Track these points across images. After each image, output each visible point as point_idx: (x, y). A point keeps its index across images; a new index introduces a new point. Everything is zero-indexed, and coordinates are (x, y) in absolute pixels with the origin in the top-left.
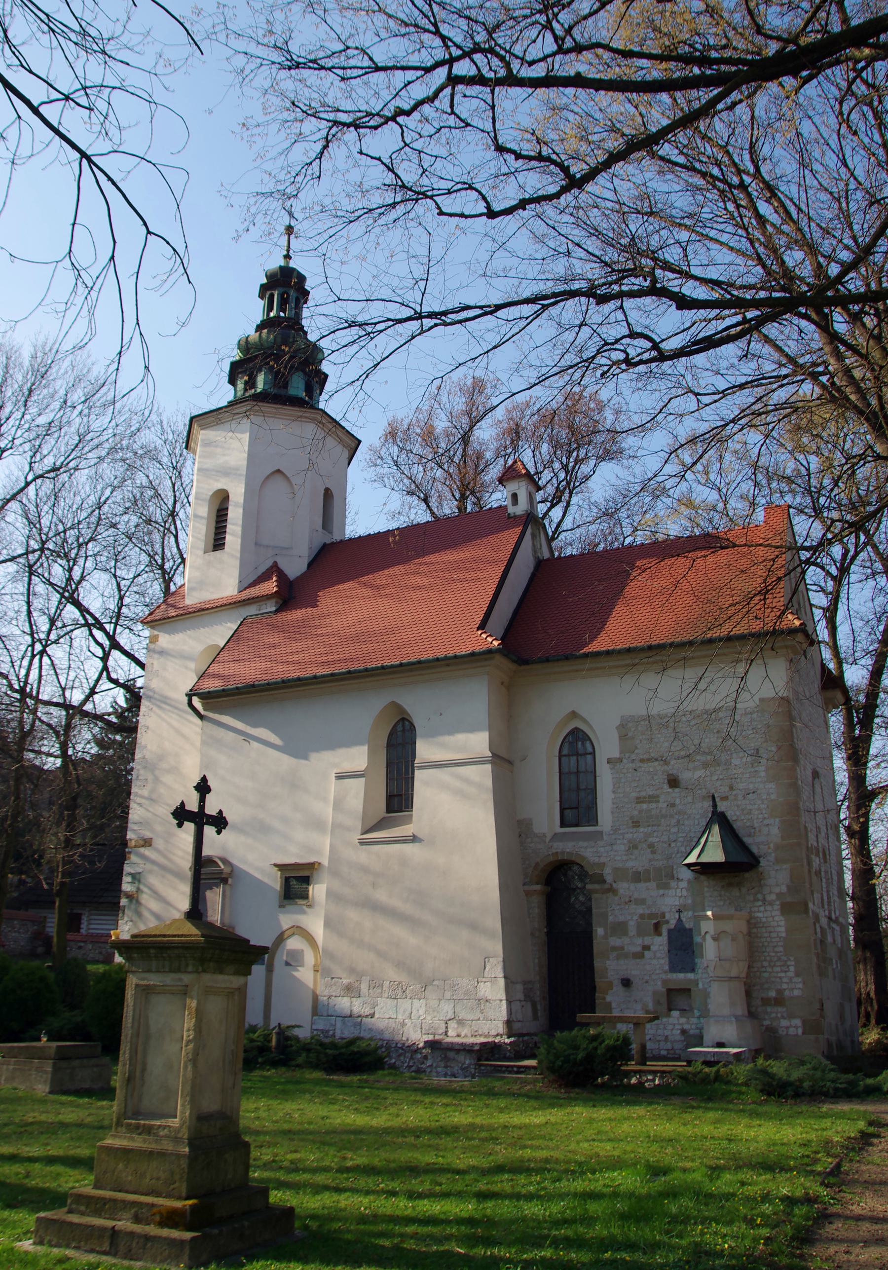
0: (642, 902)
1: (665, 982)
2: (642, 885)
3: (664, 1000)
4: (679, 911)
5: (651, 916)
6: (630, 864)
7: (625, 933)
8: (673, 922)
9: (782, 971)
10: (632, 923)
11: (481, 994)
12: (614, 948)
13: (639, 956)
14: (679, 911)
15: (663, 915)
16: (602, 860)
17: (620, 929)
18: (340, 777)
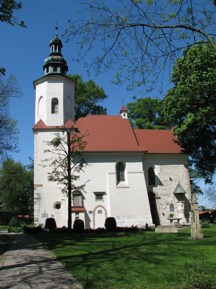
0: (164, 199)
2: (165, 196)
3: (169, 216)
6: (163, 193)
11: (147, 217)
12: (161, 208)
13: (165, 209)
17: (161, 204)
18: (109, 174)
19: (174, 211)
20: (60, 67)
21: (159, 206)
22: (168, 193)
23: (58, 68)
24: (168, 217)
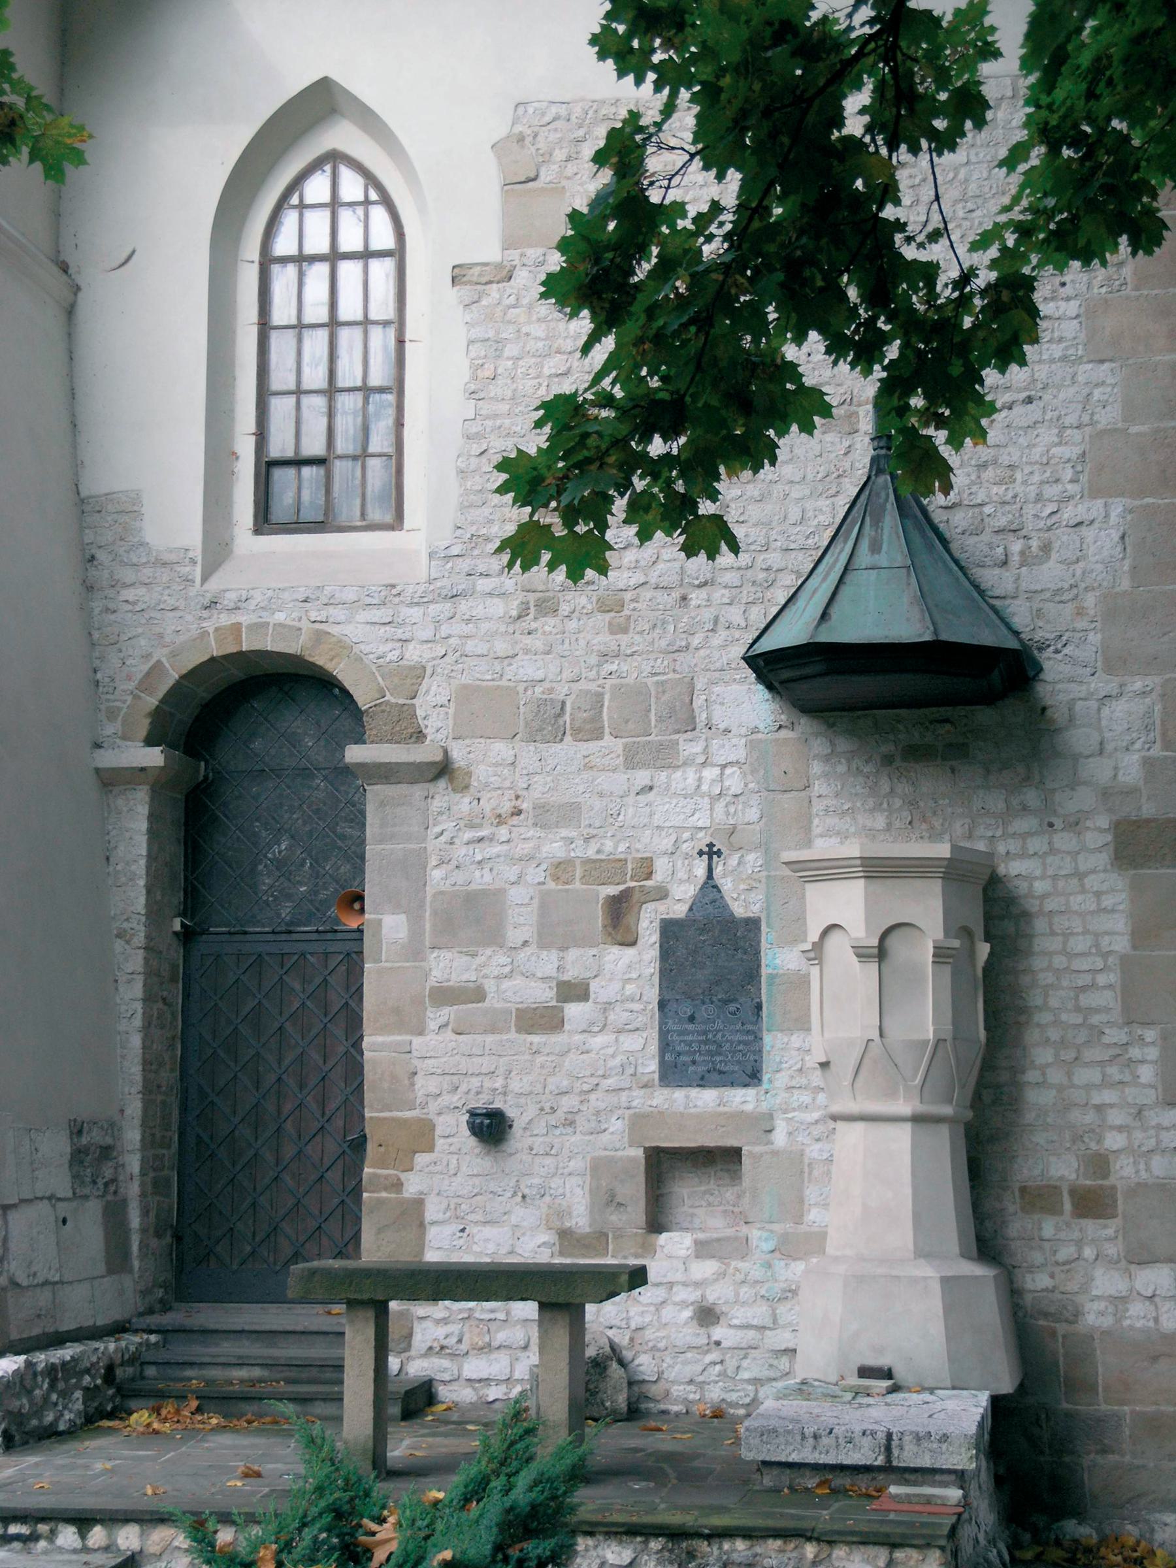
0: (570, 813)
1: (638, 1121)
2: (568, 751)
3: (635, 1190)
4: (711, 853)
5: (597, 870)
6: (527, 669)
7: (494, 936)
9: (1106, 1083)
10: (517, 895)
12: (445, 995)
14: (711, 853)
15: (646, 868)
16: (414, 654)
19: (753, 1077)
21: (415, 951)
22: (631, 670)
24: (612, 1201)
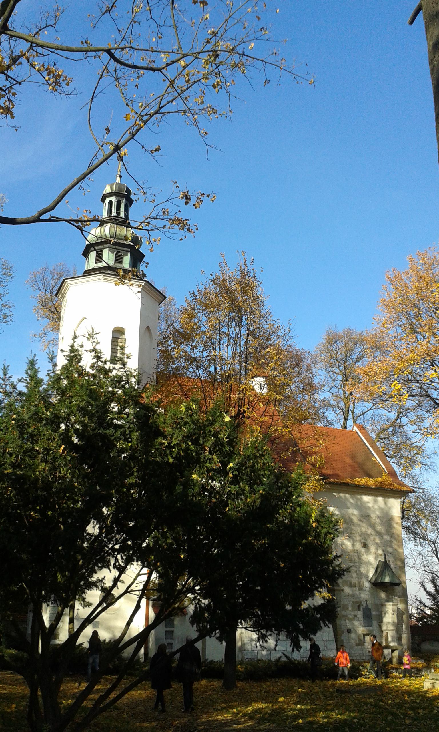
4: (366, 601)
8: (365, 605)
11: (324, 639)
15: (361, 602)
20: (129, 254)
23: (127, 255)
